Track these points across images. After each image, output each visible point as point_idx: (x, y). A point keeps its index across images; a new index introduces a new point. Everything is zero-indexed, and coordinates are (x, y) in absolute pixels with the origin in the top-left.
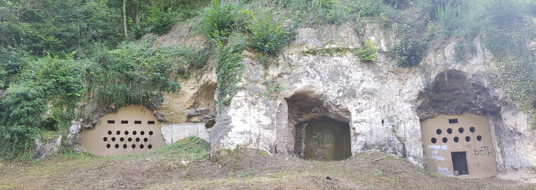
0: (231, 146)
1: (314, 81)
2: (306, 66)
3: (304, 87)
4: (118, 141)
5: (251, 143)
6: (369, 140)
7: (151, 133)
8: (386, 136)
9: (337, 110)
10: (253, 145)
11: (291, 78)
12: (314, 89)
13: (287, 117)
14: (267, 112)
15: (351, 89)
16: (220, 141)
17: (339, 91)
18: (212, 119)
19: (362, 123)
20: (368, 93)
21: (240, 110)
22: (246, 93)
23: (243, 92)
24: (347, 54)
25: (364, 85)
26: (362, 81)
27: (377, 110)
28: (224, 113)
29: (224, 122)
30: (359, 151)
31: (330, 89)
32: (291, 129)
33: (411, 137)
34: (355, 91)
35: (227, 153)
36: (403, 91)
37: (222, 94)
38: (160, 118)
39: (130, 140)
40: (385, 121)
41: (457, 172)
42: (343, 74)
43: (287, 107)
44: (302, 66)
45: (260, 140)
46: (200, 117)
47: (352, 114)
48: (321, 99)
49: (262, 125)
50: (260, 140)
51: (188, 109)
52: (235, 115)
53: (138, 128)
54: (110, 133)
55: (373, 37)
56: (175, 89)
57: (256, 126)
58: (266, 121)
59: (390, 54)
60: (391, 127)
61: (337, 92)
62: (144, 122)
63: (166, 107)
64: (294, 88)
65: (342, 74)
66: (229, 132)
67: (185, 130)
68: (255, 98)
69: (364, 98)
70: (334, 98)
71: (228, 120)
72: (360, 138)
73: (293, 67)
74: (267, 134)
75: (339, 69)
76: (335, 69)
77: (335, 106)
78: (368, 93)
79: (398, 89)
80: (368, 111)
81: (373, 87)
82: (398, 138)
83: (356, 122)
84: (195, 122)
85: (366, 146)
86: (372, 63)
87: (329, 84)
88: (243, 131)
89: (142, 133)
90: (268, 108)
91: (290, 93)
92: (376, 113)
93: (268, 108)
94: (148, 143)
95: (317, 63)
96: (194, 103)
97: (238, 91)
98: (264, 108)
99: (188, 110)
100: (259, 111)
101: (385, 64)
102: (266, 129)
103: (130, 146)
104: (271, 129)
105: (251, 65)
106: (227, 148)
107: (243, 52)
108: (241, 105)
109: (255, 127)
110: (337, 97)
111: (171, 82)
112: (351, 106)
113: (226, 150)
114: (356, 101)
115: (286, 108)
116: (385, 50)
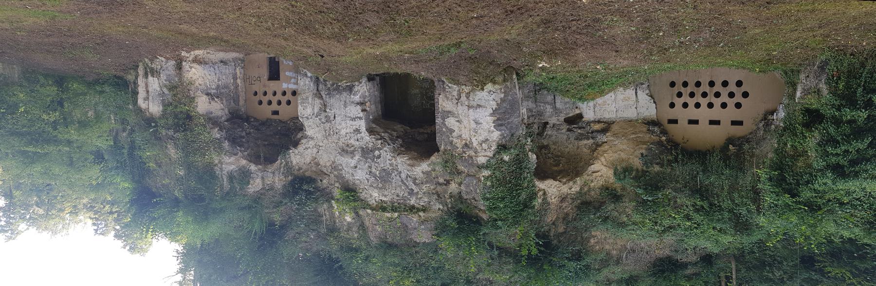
0: (492, 89)
1: (408, 172)
2: (418, 192)
4: (724, 92)
5: (467, 93)
6: (348, 96)
7: (672, 105)
9: (383, 134)
10: (465, 90)
11: (434, 178)
12: (408, 162)
14: (451, 134)
15: (366, 158)
16: (504, 96)
17: (379, 157)
18: (573, 126)
19: (354, 117)
20: (347, 152)
21: (481, 138)
22: (477, 161)
23: (479, 163)
24: (375, 204)
26: (356, 167)
28: (505, 135)
29: (503, 122)
30: (357, 84)
31: (389, 160)
34: (363, 156)
35: (495, 79)
37: (519, 162)
38: (656, 129)
39: (704, 95)
40: (332, 118)
41: (276, 60)
42: (375, 177)
43: (437, 138)
44: (424, 193)
45: (457, 97)
46: (590, 130)
47: (365, 129)
48: (402, 149)
49: (456, 117)
50: (457, 97)
51: (606, 142)
52: (489, 131)
53: (692, 112)
54: (738, 105)
55: (348, 220)
56: (623, 171)
57: (462, 115)
59: (329, 197)
60: (328, 110)
61: (381, 156)
62: (683, 122)
63: (641, 146)
64: (430, 164)
65: (377, 178)
66: (496, 108)
67: (615, 110)
68: (466, 154)
69: (352, 146)
70: (385, 148)
71: (498, 125)
72: (357, 98)
73: (434, 192)
75: (380, 185)
76: (385, 185)
77: (385, 139)
78: (347, 152)
79: (320, 153)
80: (348, 131)
81: (343, 158)
83: (360, 118)
84: (599, 122)
85: (350, 89)
86: (345, 188)
87: (390, 166)
88: (478, 109)
89: (685, 105)
90: (451, 139)
91: (434, 158)
92: (341, 127)
93: (450, 139)
94: (676, 90)
95: (406, 194)
97: (486, 164)
98: (454, 140)
99: (606, 140)
101: (332, 185)
102: (449, 112)
103: (704, 85)
104: (444, 111)
105: (477, 199)
106: (497, 86)
107: (488, 218)
108: (481, 144)
109: (463, 114)
110: (381, 149)
111: (629, 183)
112: (367, 138)
113: (498, 84)
114: (361, 144)
116: (333, 201)
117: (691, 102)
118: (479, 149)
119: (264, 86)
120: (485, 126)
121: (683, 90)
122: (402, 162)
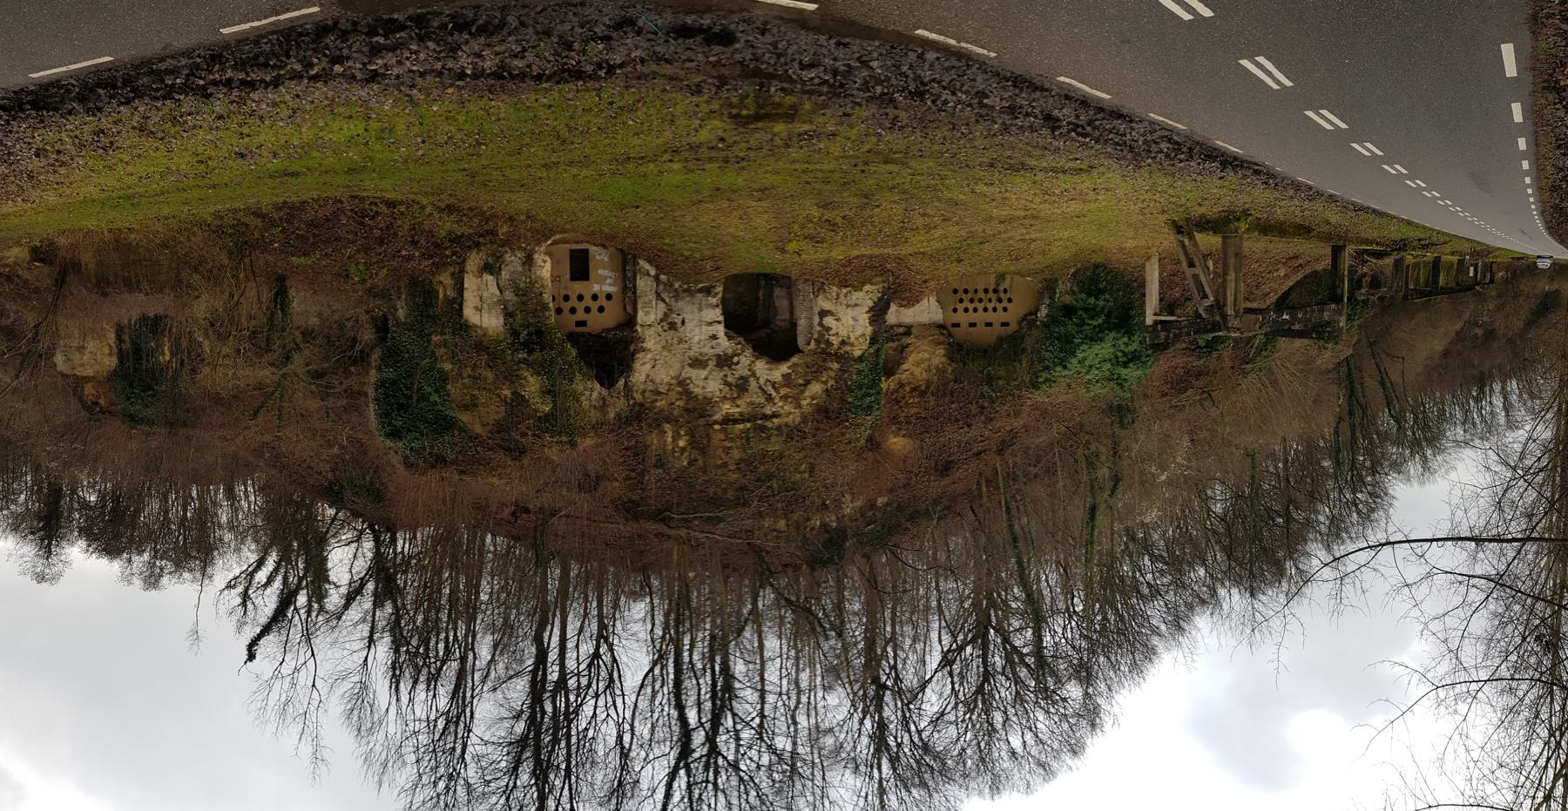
3: (778, 369)
7: (955, 310)
8: (680, 304)
12: (767, 366)
13: (799, 328)
17: (738, 363)
21: (858, 333)
25: (704, 373)
26: (706, 379)
27: (690, 339)
32: (778, 317)
33: (650, 301)
36: (648, 366)
39: (981, 300)
40: (679, 324)
53: (972, 317)
58: (828, 321)
62: (964, 325)
74: (827, 306)
75: (735, 395)
80: (702, 338)
82: (663, 300)
83: (719, 322)
94: (958, 296)
96: (902, 351)
98: (831, 338)
100: (837, 334)
112: (725, 344)
115: (801, 340)
117: (971, 307)
118: (856, 343)
119: (566, 288)
120: (861, 322)
121: (964, 296)
122: (761, 366)
